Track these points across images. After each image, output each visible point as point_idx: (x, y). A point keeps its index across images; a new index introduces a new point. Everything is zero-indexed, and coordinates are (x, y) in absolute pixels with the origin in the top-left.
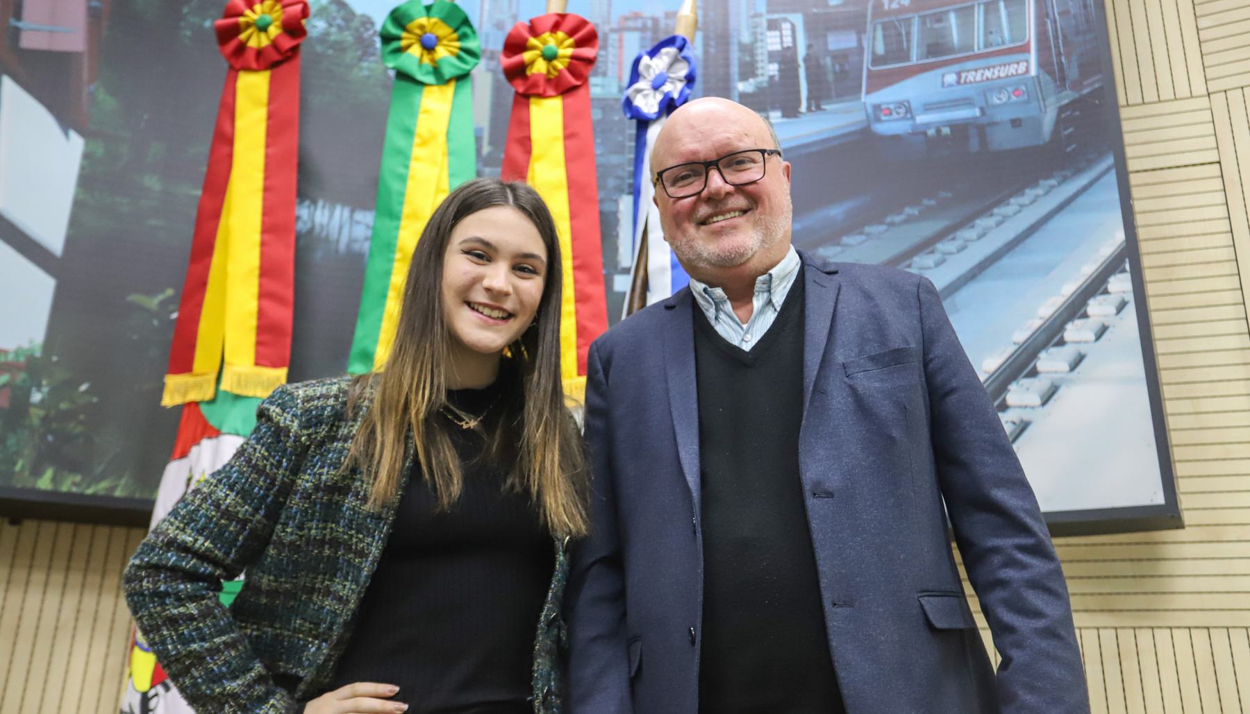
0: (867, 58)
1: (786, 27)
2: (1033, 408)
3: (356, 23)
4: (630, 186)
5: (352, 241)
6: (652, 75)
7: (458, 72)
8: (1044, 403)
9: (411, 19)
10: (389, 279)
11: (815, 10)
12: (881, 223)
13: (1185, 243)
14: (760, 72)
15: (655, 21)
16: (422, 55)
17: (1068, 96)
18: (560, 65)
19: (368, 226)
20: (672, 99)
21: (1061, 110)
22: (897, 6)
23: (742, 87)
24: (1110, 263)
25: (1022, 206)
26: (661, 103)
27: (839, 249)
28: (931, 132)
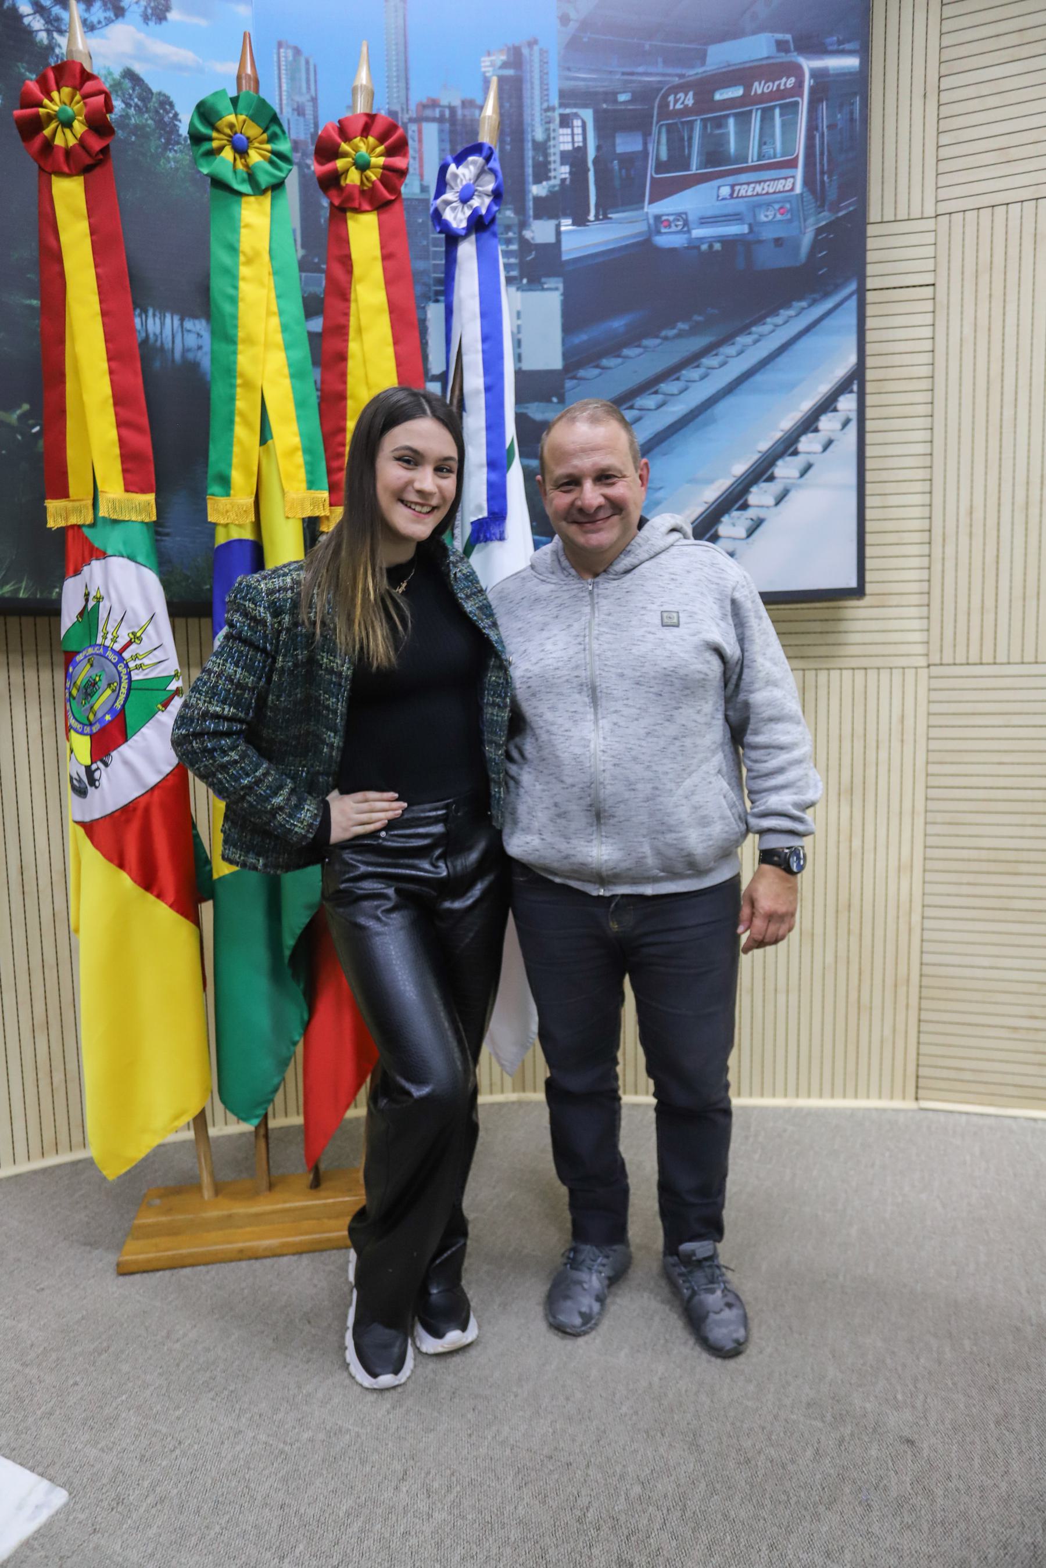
0: (651, 164)
1: (577, 123)
2: (768, 507)
3: (153, 103)
4: (437, 293)
5: (185, 350)
6: (459, 188)
7: (273, 181)
8: (777, 503)
9: (220, 119)
10: (234, 405)
11: (605, 106)
12: (657, 337)
13: (897, 360)
14: (552, 174)
15: (452, 110)
16: (235, 159)
17: (826, 217)
18: (373, 176)
19: (199, 335)
20: (481, 216)
21: (819, 231)
22: (682, 106)
23: (537, 190)
24: (841, 385)
25: (777, 326)
26: (470, 219)
27: (619, 360)
28: (704, 247)
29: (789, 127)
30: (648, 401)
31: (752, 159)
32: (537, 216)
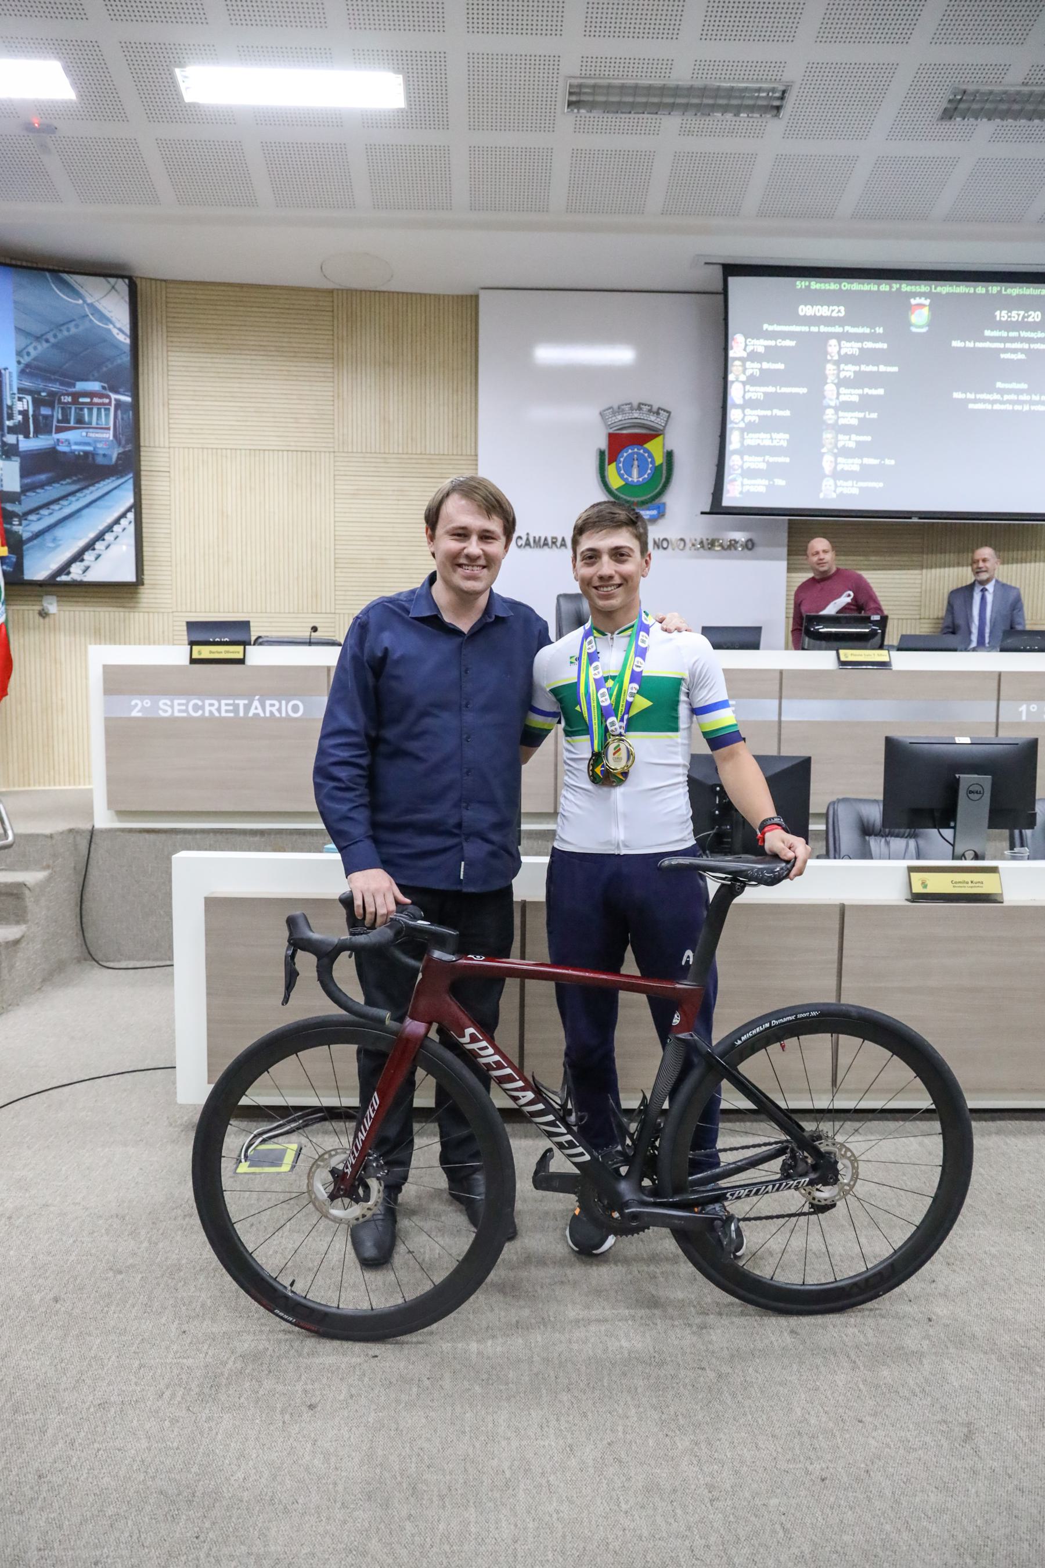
1: (24, 400)
17: (121, 450)
21: (119, 454)
23: (8, 423)
28: (77, 453)
29: (107, 415)
30: (56, 507)
31: (94, 424)
32: (8, 433)
